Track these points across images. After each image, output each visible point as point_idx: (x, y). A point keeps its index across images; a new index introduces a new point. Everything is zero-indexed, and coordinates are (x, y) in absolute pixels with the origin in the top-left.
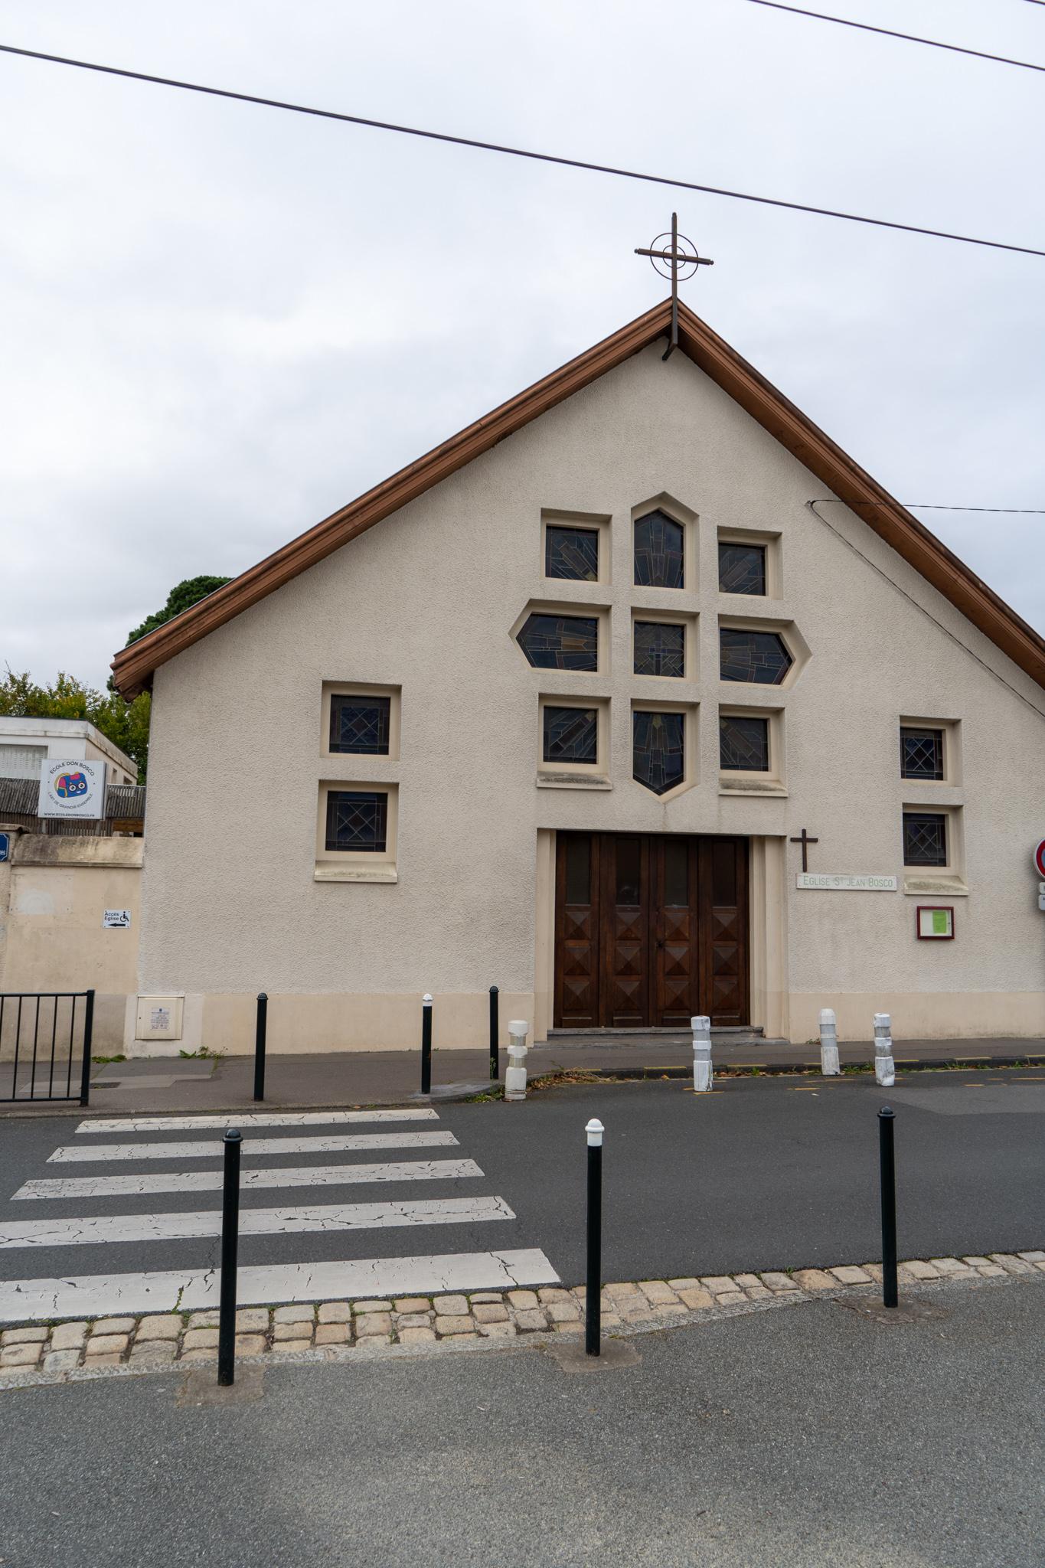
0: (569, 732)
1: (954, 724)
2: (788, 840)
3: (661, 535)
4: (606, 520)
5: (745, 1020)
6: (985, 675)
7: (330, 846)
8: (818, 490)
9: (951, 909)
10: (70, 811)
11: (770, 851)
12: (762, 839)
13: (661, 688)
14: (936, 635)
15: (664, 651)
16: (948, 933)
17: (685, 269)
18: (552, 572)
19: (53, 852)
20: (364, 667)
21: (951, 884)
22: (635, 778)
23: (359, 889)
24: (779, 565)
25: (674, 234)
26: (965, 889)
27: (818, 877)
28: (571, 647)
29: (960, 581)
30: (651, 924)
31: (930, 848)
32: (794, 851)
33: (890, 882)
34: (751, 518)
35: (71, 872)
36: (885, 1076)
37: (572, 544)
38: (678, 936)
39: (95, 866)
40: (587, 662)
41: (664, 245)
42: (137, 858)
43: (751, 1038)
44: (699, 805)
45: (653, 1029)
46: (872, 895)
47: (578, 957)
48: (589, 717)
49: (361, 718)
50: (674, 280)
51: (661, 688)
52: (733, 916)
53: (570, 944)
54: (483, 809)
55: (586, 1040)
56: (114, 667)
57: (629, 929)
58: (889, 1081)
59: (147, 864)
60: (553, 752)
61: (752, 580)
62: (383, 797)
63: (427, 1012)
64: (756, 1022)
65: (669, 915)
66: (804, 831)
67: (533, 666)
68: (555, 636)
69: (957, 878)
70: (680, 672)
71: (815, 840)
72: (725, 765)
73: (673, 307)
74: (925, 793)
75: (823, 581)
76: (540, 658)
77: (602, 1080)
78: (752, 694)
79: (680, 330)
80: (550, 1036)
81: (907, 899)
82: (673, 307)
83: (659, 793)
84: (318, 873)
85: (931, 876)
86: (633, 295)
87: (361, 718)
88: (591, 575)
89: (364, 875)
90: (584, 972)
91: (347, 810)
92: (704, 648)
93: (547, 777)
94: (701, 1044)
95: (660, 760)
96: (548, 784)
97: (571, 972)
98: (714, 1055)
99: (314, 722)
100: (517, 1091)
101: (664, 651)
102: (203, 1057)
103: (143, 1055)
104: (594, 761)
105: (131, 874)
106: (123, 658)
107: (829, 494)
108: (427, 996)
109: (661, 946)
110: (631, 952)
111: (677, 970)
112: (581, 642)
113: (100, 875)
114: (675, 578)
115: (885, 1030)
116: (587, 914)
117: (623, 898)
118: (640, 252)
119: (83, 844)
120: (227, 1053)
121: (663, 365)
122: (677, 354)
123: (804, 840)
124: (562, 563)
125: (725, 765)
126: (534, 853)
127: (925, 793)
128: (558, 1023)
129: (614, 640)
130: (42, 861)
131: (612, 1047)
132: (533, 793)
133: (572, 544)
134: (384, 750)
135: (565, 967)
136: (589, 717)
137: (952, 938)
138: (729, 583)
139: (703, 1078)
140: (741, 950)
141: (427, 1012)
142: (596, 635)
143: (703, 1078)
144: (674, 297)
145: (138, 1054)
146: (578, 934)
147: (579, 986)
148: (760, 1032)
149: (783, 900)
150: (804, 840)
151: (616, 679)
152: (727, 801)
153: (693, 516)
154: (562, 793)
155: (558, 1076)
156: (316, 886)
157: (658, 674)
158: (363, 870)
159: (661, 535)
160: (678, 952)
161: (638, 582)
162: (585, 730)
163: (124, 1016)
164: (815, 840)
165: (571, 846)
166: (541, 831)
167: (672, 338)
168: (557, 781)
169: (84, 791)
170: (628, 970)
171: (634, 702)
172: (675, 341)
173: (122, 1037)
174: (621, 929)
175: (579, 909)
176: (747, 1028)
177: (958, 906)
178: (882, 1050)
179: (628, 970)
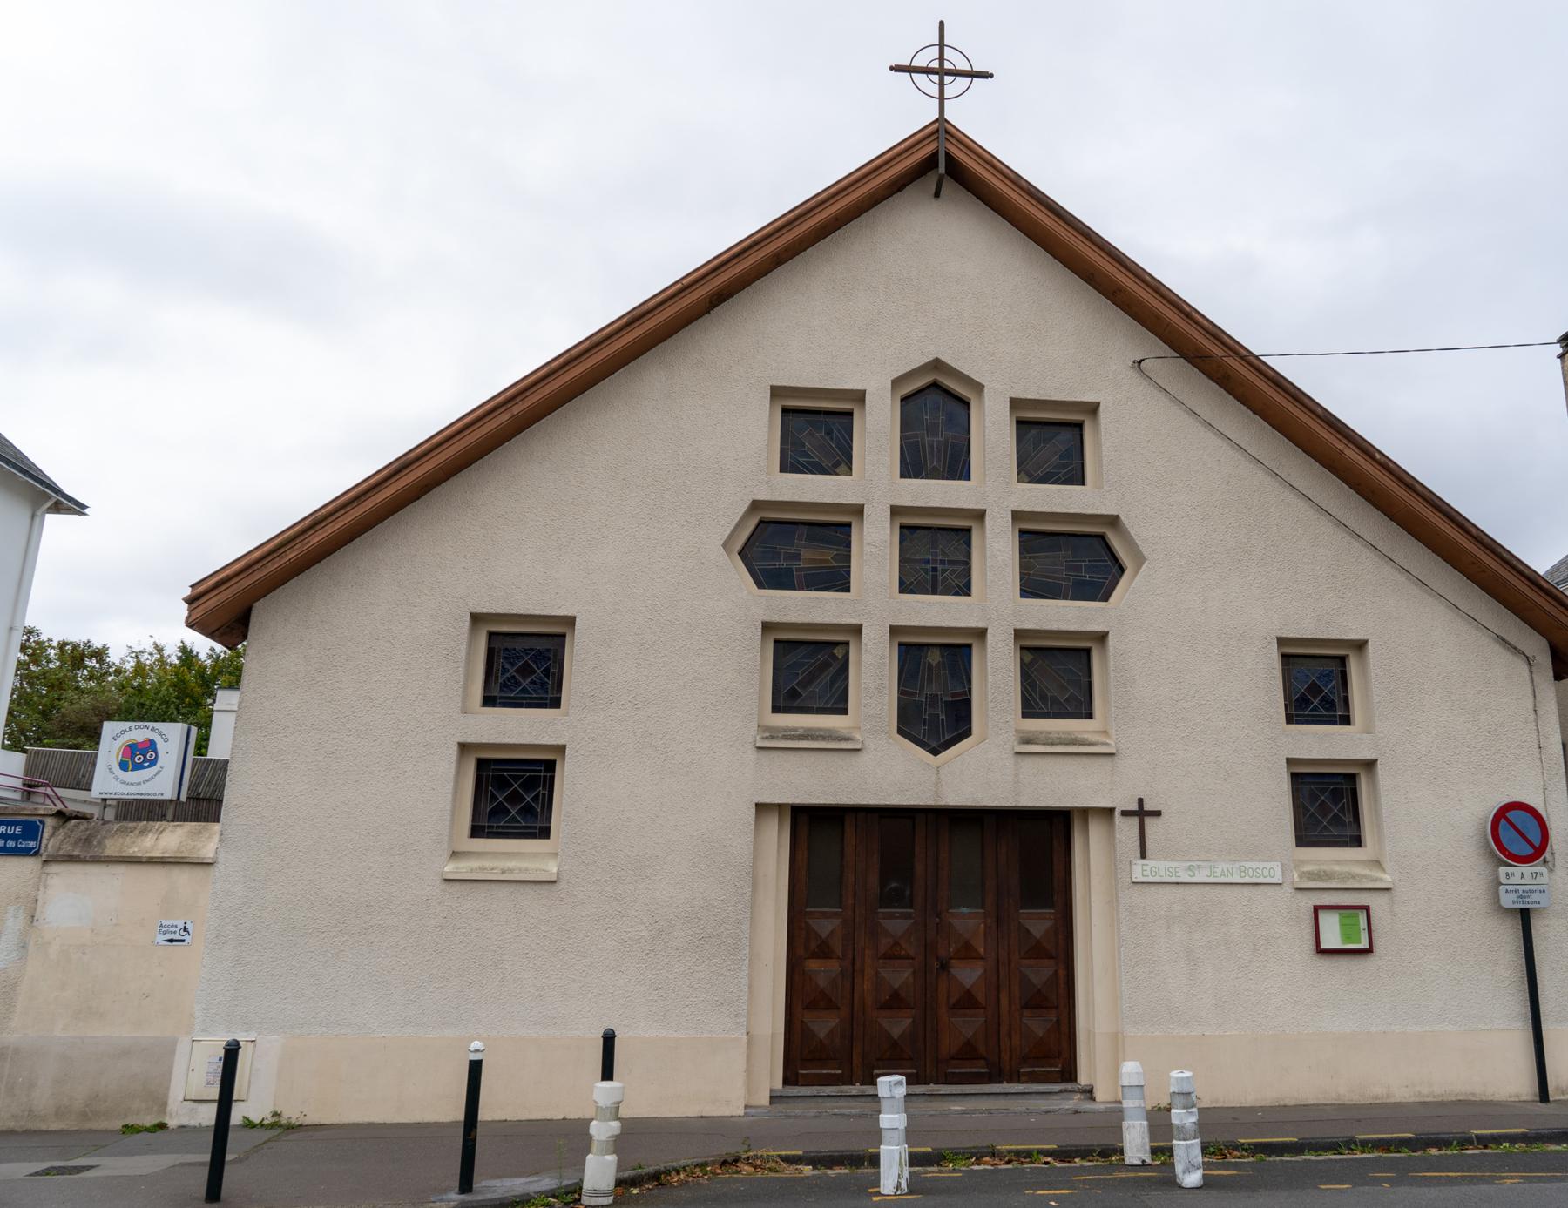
0: (807, 673)
1: (1360, 646)
2: (1117, 813)
3: (936, 416)
4: (859, 397)
5: (1069, 1074)
6: (1401, 578)
7: (476, 831)
8: (1148, 346)
9: (1367, 909)
10: (133, 789)
11: (1096, 830)
12: (1085, 812)
13: (936, 612)
14: (1325, 526)
15: (942, 562)
16: (1364, 944)
17: (954, 86)
18: (789, 464)
19: (99, 843)
20: (525, 593)
21: (1366, 872)
22: (900, 732)
23: (504, 891)
24: (1098, 445)
25: (941, 45)
26: (1387, 879)
27: (1162, 865)
28: (814, 560)
29: (1348, 452)
30: (934, 938)
31: (1336, 821)
32: (1126, 830)
33: (1272, 870)
34: (1057, 383)
35: (120, 869)
36: (1187, 1171)
37: (815, 428)
38: (967, 952)
39: (151, 862)
40: (837, 579)
41: (928, 58)
42: (208, 850)
43: (1075, 1102)
44: (992, 767)
45: (932, 1088)
46: (1246, 891)
47: (822, 982)
48: (839, 652)
49: (524, 662)
51: (936, 612)
52: (1048, 924)
53: (813, 965)
54: (686, 780)
55: (829, 1103)
56: (190, 601)
57: (896, 943)
58: (1192, 1179)
59: (221, 858)
60: (785, 700)
61: (1065, 466)
62: (550, 766)
63: (475, 1068)
64: (1083, 1080)
65: (955, 922)
66: (1141, 801)
67: (760, 585)
68: (792, 548)
69: (1377, 863)
70: (965, 590)
71: (1158, 814)
72: (1029, 711)
73: (941, 129)
74: (1322, 743)
75: (1157, 464)
76: (769, 577)
77: (789, 1171)
78: (1063, 615)
79: (948, 156)
80: (774, 1098)
81: (1300, 895)
82: (941, 129)
84: (450, 869)
85: (1338, 862)
86: (893, 118)
87: (524, 662)
88: (843, 467)
89: (511, 871)
90: (830, 1005)
91: (502, 783)
92: (996, 556)
93: (772, 733)
94: (892, 1120)
96: (771, 744)
97: (811, 1006)
98: (911, 1134)
99: (465, 664)
100: (596, 1193)
101: (942, 562)
102: (272, 1126)
103: (193, 1123)
104: (845, 711)
105: (199, 873)
106: (200, 589)
107: (1165, 350)
108: (476, 1045)
109: (944, 967)
110: (900, 977)
111: (967, 1002)
112: (828, 555)
113: (157, 873)
114: (956, 465)
115: (1185, 1098)
116: (837, 922)
117: (890, 899)
118: (897, 69)
119: (143, 832)
120: (307, 1121)
121: (935, 204)
122: (949, 187)
123: (1141, 813)
124: (805, 454)
125: (1029, 711)
126: (750, 838)
127: (1322, 743)
128: (791, 1077)
129: (867, 548)
130: (86, 854)
131: (860, 1116)
132: (751, 755)
133: (815, 428)
134: (556, 703)
135: (802, 996)
136: (839, 652)
137: (1368, 951)
138: (1030, 470)
139: (892, 1173)
140: (1062, 973)
141: (475, 1068)
142: (849, 545)
143: (892, 1173)
144: (941, 119)
145: (185, 1121)
146: (824, 951)
147: (824, 1025)
148: (1089, 1092)
149: (1113, 901)
150: (1141, 813)
151: (874, 601)
152: (1028, 761)
153: (979, 388)
154: (791, 755)
155: (728, 1162)
156: (446, 886)
157: (934, 592)
158: (511, 864)
159: (936, 416)
160: (968, 975)
161: (905, 474)
162: (832, 670)
163: (171, 1067)
164: (1158, 814)
165: (812, 825)
166: (762, 808)
167: (941, 167)
168: (785, 738)
169: (153, 763)
170: (895, 1002)
171: (895, 631)
173: (166, 1096)
174: (885, 943)
175: (824, 915)
176: (1069, 1086)
177: (1377, 903)
178: (1181, 1128)
179: (895, 1002)
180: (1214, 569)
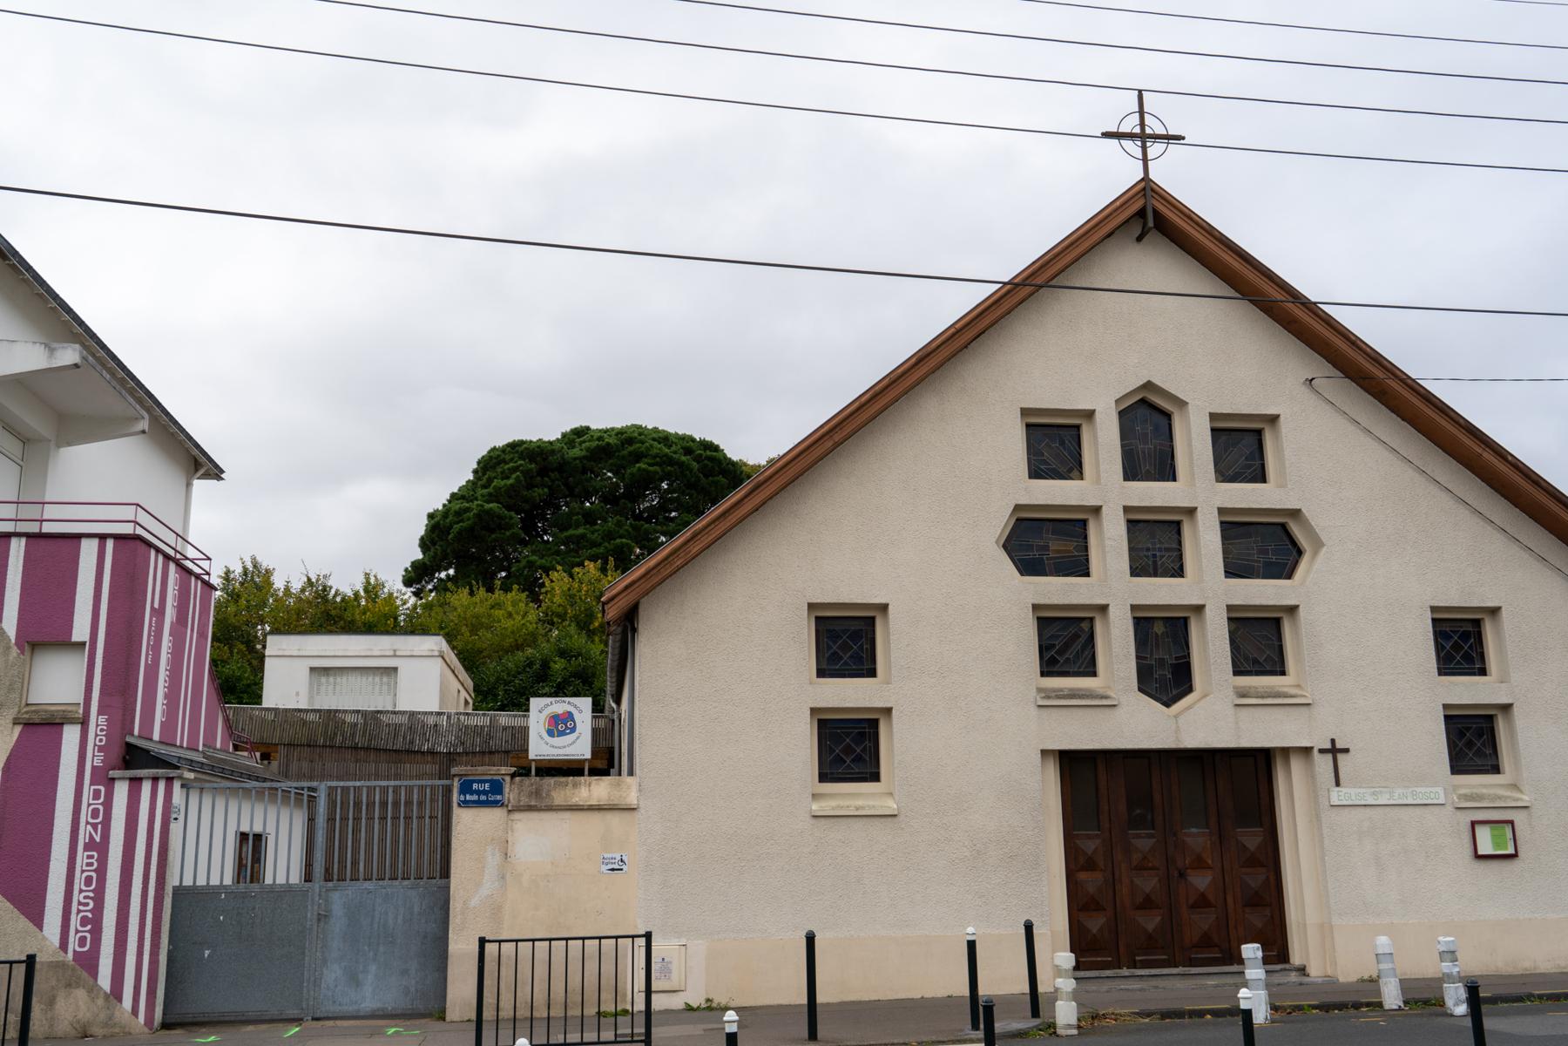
0: (1065, 644)
1: (1494, 611)
2: (1315, 751)
3: (1148, 427)
4: (1089, 415)
6: (1525, 555)
7: (823, 778)
8: (1317, 367)
9: (1512, 822)
11: (1296, 764)
12: (1286, 752)
13: (1161, 592)
14: (1463, 513)
15: (1160, 550)
16: (1511, 851)
17: (1154, 149)
18: (1036, 473)
20: (848, 587)
21: (1508, 793)
22: (1140, 690)
23: (859, 823)
24: (1279, 450)
25: (1141, 112)
26: (1525, 799)
27: (1353, 791)
28: (1058, 551)
29: (1485, 455)
30: (1173, 851)
31: (1479, 753)
32: (1323, 764)
33: (1437, 794)
34: (1244, 401)
35: (567, 815)
36: (1456, 1004)
37: (1054, 443)
38: (1200, 864)
39: (591, 808)
40: (1080, 567)
42: (632, 798)
44: (1213, 716)
46: (1418, 810)
48: (1085, 625)
49: (846, 640)
50: (1145, 160)
51: (1161, 592)
52: (1259, 839)
53: (1082, 876)
60: (1050, 666)
61: (1250, 466)
62: (874, 724)
63: (972, 946)
64: (1296, 959)
65: (1188, 840)
66: (1333, 741)
68: (1046, 542)
69: (1515, 786)
70: (1179, 572)
71: (1346, 751)
72: (1238, 672)
73: (1146, 188)
74: (1467, 691)
75: (1328, 463)
76: (1029, 566)
78: (1261, 592)
79: (1156, 212)
81: (1459, 813)
82: (1146, 188)
83: (1168, 705)
84: (816, 807)
85: (1485, 786)
87: (846, 640)
92: (1204, 545)
95: (1165, 666)
96: (1049, 702)
100: (1069, 1026)
101: (1160, 550)
102: (710, 1009)
105: (626, 815)
107: (1328, 369)
108: (970, 930)
109: (1182, 875)
110: (1149, 884)
111: (1202, 902)
112: (1071, 546)
114: (1166, 470)
115: (1450, 955)
116: (1098, 842)
119: (575, 785)
121: (1138, 247)
122: (1154, 236)
123: (1334, 751)
124: (1045, 462)
125: (1238, 672)
127: (1467, 691)
129: (1108, 542)
132: (1034, 711)
134: (872, 673)
136: (1085, 625)
137: (1514, 856)
138: (1228, 471)
140: (1272, 878)
141: (972, 946)
144: (1146, 178)
146: (1090, 865)
147: (1095, 923)
148: (1302, 970)
149: (1316, 818)
150: (1334, 751)
151: (1111, 585)
152: (1245, 711)
153: (1182, 404)
154: (1064, 711)
156: (813, 821)
157: (1155, 575)
158: (860, 803)
159: (1148, 427)
160: (1201, 881)
161: (1126, 478)
162: (1082, 640)
164: (1346, 751)
165: (1076, 768)
166: (1044, 753)
167: (1149, 218)
168: (1058, 697)
169: (573, 730)
170: (1147, 904)
172: (1151, 224)
175: (1089, 837)
177: (1519, 818)
179: (1147, 904)
180: (1379, 553)
